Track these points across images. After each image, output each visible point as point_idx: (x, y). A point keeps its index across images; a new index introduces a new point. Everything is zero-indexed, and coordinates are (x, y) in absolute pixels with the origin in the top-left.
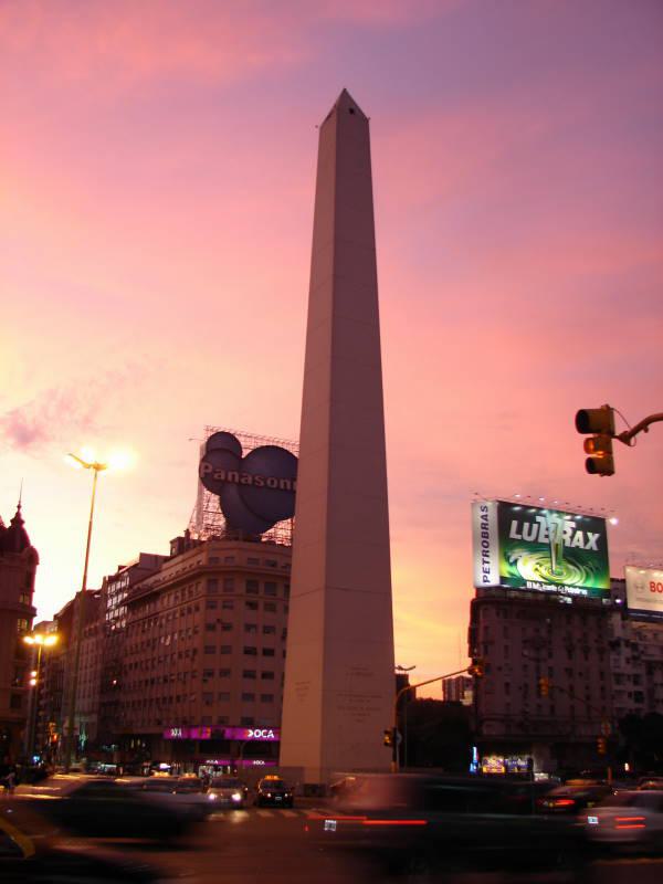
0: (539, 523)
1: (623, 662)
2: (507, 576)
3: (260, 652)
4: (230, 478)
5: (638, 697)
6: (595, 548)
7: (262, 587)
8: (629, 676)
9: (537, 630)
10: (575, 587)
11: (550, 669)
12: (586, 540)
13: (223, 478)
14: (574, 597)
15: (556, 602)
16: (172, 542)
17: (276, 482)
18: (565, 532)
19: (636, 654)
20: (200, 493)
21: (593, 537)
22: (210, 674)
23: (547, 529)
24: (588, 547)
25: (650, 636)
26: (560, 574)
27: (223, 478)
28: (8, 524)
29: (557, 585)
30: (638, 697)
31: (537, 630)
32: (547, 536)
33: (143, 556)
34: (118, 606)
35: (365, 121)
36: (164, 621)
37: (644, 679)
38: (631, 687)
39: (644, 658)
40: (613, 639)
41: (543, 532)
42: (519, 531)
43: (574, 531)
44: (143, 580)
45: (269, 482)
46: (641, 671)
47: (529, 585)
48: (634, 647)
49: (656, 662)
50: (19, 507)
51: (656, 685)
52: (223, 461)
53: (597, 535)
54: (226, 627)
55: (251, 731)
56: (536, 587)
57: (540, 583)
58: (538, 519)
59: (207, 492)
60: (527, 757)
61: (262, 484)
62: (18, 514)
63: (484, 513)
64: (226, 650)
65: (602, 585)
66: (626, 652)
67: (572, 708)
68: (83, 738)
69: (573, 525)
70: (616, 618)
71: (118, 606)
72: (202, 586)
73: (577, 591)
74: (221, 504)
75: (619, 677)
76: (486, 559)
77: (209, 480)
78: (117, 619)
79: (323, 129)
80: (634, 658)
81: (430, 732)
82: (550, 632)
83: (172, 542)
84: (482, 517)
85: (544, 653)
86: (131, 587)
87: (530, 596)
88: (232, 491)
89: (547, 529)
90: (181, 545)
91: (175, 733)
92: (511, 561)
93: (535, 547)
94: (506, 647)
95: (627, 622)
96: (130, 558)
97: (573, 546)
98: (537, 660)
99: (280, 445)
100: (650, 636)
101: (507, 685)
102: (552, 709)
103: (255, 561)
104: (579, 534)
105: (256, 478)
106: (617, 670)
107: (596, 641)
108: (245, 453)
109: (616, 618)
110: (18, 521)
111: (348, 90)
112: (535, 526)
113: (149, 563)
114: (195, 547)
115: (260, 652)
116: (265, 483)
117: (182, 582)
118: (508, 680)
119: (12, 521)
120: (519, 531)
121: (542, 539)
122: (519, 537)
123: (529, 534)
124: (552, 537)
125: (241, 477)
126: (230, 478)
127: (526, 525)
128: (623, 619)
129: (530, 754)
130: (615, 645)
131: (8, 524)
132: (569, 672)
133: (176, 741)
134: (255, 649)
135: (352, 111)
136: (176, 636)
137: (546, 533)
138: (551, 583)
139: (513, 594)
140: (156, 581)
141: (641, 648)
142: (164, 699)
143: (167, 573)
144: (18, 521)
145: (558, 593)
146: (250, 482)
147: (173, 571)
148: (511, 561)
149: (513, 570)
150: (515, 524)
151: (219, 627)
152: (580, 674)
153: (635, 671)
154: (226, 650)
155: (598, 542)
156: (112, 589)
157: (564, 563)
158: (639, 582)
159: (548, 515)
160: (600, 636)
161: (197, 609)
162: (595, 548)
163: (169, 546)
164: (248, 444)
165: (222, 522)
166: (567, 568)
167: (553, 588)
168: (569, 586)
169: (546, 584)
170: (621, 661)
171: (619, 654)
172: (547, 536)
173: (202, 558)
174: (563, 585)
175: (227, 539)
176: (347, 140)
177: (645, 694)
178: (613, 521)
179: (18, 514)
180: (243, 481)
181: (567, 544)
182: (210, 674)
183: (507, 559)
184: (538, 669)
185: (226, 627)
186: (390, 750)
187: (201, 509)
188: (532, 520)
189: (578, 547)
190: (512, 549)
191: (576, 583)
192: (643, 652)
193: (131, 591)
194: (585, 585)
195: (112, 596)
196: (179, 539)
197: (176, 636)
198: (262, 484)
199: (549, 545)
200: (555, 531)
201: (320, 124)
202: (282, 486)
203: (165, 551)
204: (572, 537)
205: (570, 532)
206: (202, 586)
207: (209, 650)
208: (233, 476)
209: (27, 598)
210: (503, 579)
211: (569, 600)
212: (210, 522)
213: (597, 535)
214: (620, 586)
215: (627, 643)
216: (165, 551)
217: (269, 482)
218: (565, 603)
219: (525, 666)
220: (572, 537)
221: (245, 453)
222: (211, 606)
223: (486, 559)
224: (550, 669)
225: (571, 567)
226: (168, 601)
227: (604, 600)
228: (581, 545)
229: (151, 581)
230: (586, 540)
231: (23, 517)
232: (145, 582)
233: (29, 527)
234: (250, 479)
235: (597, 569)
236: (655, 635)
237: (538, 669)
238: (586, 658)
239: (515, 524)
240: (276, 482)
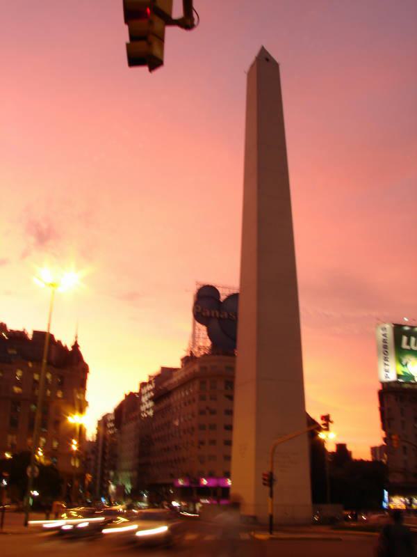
2: (402, 374)
4: (213, 315)
20: (194, 325)
22: (202, 443)
28: (70, 349)
33: (163, 369)
34: (148, 401)
35: (276, 66)
42: (408, 343)
50: (76, 337)
52: (210, 307)
54: (213, 412)
59: (198, 324)
62: (76, 343)
63: (383, 332)
64: (213, 427)
68: (129, 487)
72: (197, 382)
74: (209, 335)
76: (387, 363)
77: (199, 316)
78: (148, 409)
79: (249, 74)
81: (338, 479)
90: (187, 360)
91: (181, 482)
96: (155, 370)
105: (231, 315)
108: (223, 298)
110: (76, 346)
111: (265, 48)
113: (166, 373)
117: (184, 384)
119: (73, 347)
120: (408, 343)
125: (220, 313)
126: (213, 315)
131: (70, 349)
133: (182, 487)
135: (267, 60)
136: (182, 420)
139: (406, 386)
142: (175, 460)
143: (176, 379)
144: (76, 346)
147: (179, 377)
149: (405, 370)
150: (405, 339)
151: (207, 412)
154: (213, 427)
156: (144, 391)
161: (194, 400)
165: (208, 343)
173: (196, 367)
175: (213, 354)
176: (265, 78)
179: (76, 343)
180: (222, 316)
182: (202, 443)
185: (213, 412)
186: (267, 489)
187: (194, 336)
190: (407, 354)
195: (144, 395)
197: (182, 420)
201: (247, 67)
203: (176, 364)
206: (197, 382)
207: (202, 427)
208: (215, 314)
209: (82, 395)
210: (399, 376)
212: (201, 344)
216: (176, 364)
221: (223, 298)
222: (202, 398)
223: (387, 363)
226: (177, 397)
229: (166, 384)
231: (79, 343)
233: (82, 350)
234: (226, 315)
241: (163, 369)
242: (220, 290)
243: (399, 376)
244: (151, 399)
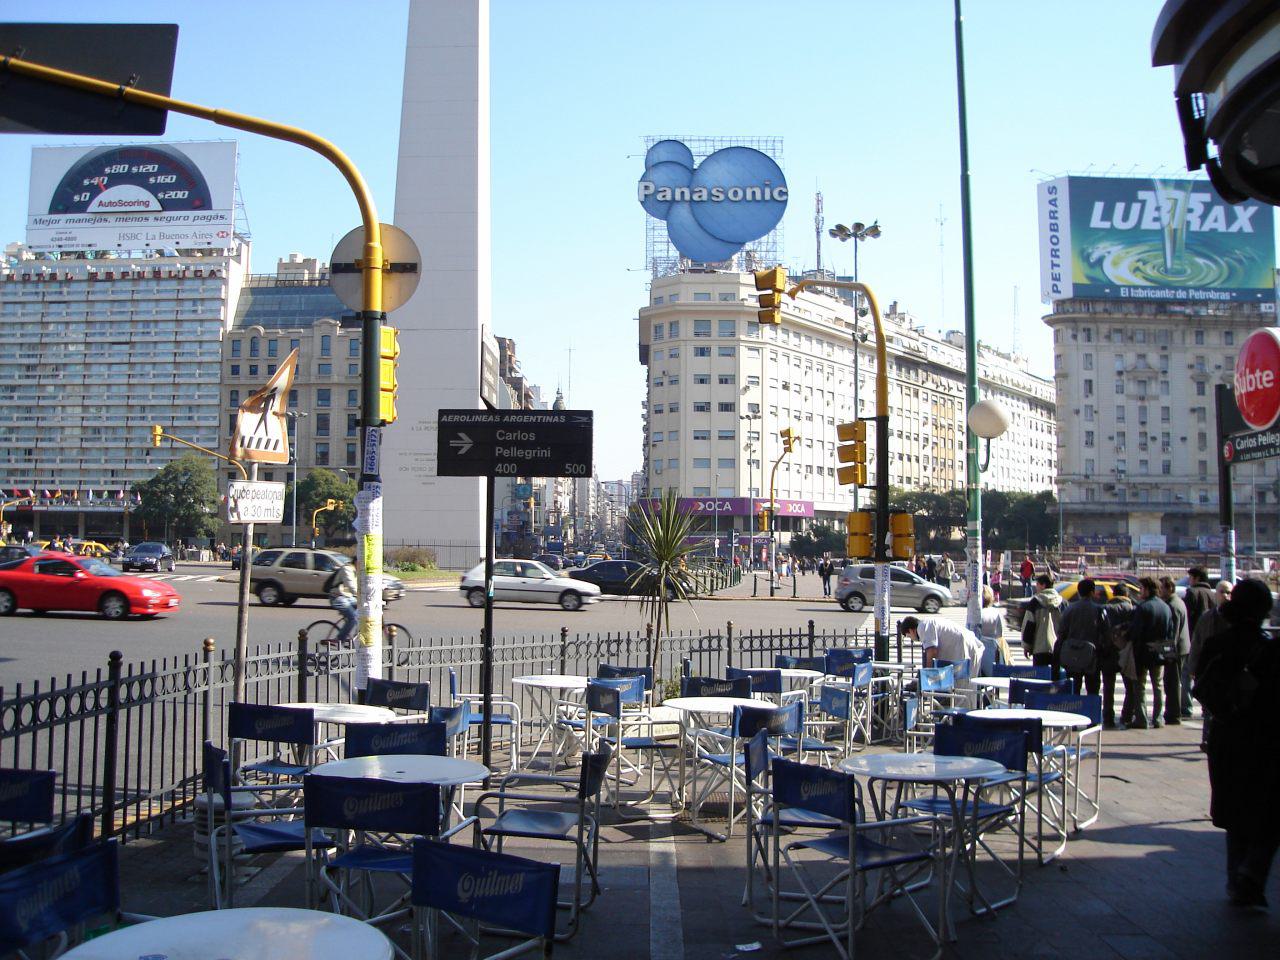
0: (1143, 203)
4: (678, 197)
6: (1248, 229)
7: (715, 328)
11: (1166, 409)
13: (669, 198)
17: (740, 193)
18: (1190, 211)
23: (1158, 209)
24: (1234, 228)
27: (669, 198)
31: (1142, 356)
32: (1156, 219)
45: (731, 195)
47: (1123, 293)
61: (722, 197)
63: (1053, 197)
76: (1056, 261)
77: (653, 204)
84: (1050, 202)
85: (1154, 388)
88: (682, 213)
89: (1158, 209)
94: (1089, 383)
97: (1206, 228)
101: (1090, 434)
103: (708, 296)
105: (714, 192)
108: (698, 161)
116: (725, 193)
118: (1090, 427)
121: (1148, 224)
122: (1107, 225)
123: (1125, 218)
124: (1165, 218)
126: (678, 197)
137: (1156, 214)
138: (1162, 286)
146: (705, 198)
149: (1096, 273)
155: (1252, 219)
162: (1248, 229)
164: (703, 149)
167: (1166, 294)
169: (1152, 288)
172: (1156, 219)
174: (1186, 289)
180: (696, 197)
181: (1195, 227)
184: (1143, 410)
189: (1213, 231)
190: (1101, 239)
194: (1226, 286)
198: (722, 197)
199: (1161, 231)
202: (749, 197)
205: (1199, 210)
217: (731, 195)
219: (1121, 408)
220: (1203, 217)
221: (698, 161)
223: (1056, 261)
224: (1166, 409)
228: (1221, 227)
230: (1231, 218)
237: (1143, 410)
239: (1099, 207)
240: (740, 193)
242: (694, 148)
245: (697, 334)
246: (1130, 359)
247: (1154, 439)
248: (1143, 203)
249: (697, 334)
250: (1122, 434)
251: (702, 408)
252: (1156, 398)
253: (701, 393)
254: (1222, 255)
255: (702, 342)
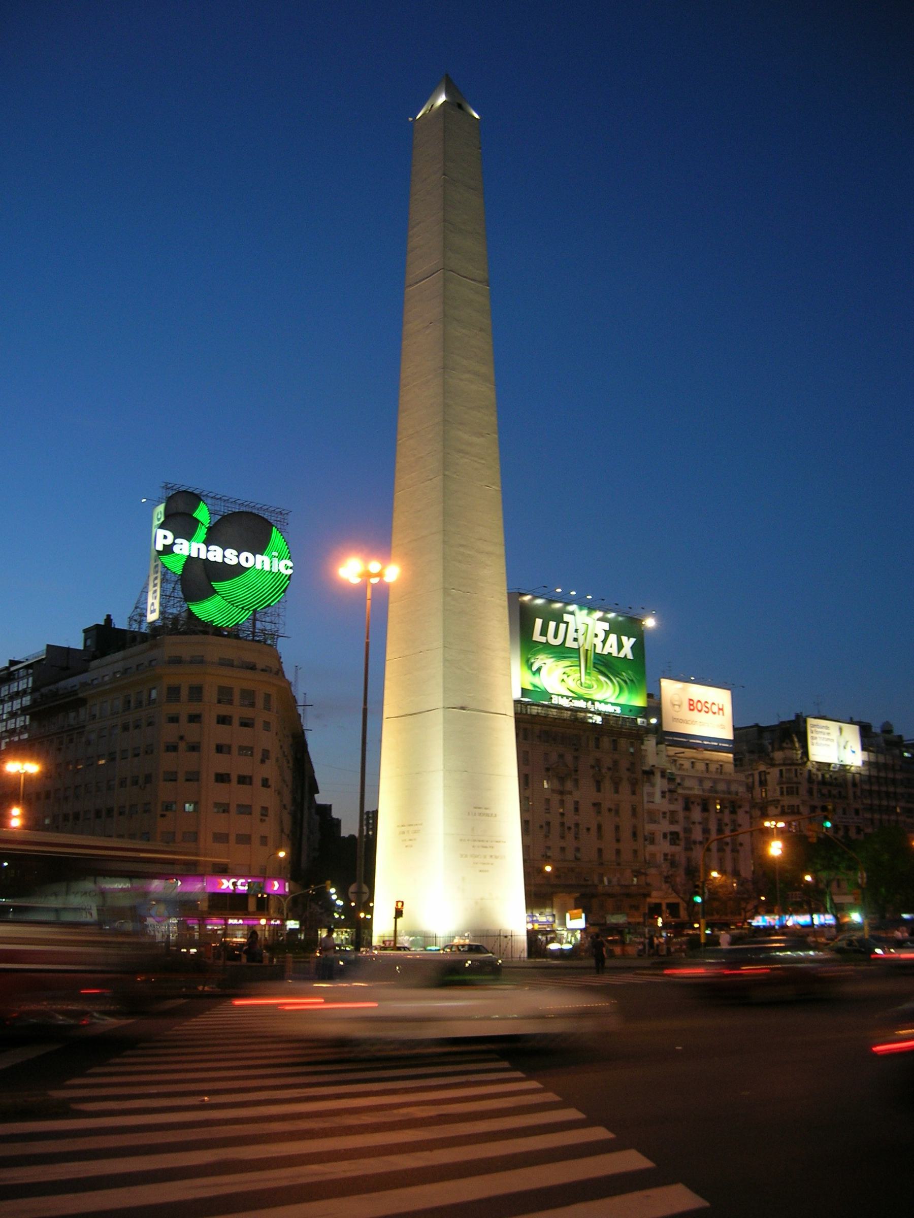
0: (567, 623)
1: (658, 795)
2: (531, 688)
3: (234, 779)
5: (674, 838)
6: (630, 656)
8: (664, 813)
9: (561, 756)
10: (606, 703)
12: (620, 646)
14: (606, 716)
15: (584, 722)
16: (85, 631)
19: (672, 787)
21: (628, 642)
23: (576, 631)
24: (622, 655)
25: (687, 764)
26: (590, 687)
29: (587, 700)
30: (674, 838)
32: (575, 640)
33: (49, 647)
36: (93, 736)
37: (681, 815)
38: (665, 826)
39: (680, 791)
40: (646, 768)
41: (571, 634)
42: (544, 632)
43: (607, 633)
44: (57, 682)
46: (678, 806)
47: (555, 700)
48: (671, 779)
49: (696, 796)
51: (694, 823)
53: (633, 640)
54: (194, 748)
55: (224, 881)
56: (565, 703)
57: (568, 697)
58: (566, 617)
60: (548, 910)
65: (639, 701)
66: (660, 784)
67: (600, 851)
69: (606, 626)
70: (650, 744)
71: (13, 715)
73: (609, 709)
75: (652, 817)
80: (670, 791)
82: (576, 758)
83: (86, 631)
85: (569, 785)
86: (35, 689)
87: (554, 712)
89: (576, 631)
92: (535, 668)
93: (561, 652)
95: (662, 747)
97: (605, 652)
98: (562, 793)
99: (256, 512)
100: (687, 764)
102: (578, 849)
104: (613, 638)
106: (651, 806)
107: (628, 770)
109: (650, 744)
112: (562, 627)
114: (143, 642)
115: (234, 779)
120: (544, 632)
121: (570, 643)
123: (556, 636)
124: (581, 639)
127: (552, 625)
128: (657, 744)
129: (552, 907)
130: (650, 773)
132: (597, 805)
134: (228, 775)
138: (579, 698)
139: (535, 710)
140: (84, 685)
141: (678, 780)
145: (586, 710)
148: (535, 668)
149: (536, 680)
150: (539, 622)
152: (610, 810)
153: (672, 807)
155: (633, 648)
157: (594, 673)
158: (676, 698)
159: (577, 612)
160: (632, 764)
162: (630, 656)
163: (82, 636)
166: (598, 680)
167: (581, 704)
168: (600, 702)
170: (655, 794)
171: (653, 785)
172: (575, 640)
177: (682, 835)
178: (650, 623)
181: (598, 651)
183: (530, 666)
185: (194, 748)
188: (559, 619)
190: (538, 652)
191: (609, 698)
192: (679, 784)
193: (37, 695)
196: (97, 626)
200: (585, 634)
204: (604, 642)
205: (602, 636)
210: (524, 692)
211: (598, 719)
213: (633, 640)
214: (654, 707)
215: (663, 774)
216: (77, 642)
218: (595, 724)
220: (604, 642)
224: (577, 803)
225: (602, 678)
227: (639, 720)
228: (615, 654)
230: (620, 646)
232: (62, 684)
235: (632, 681)
236: (693, 763)
238: (617, 792)
241: (49, 647)
243: (524, 692)
244: (24, 710)
245: (219, 702)
246: (554, 757)
247: (569, 828)
248: (567, 623)
249: (219, 702)
250: (548, 824)
251: (222, 778)
252: (570, 793)
253: (221, 763)
254: (615, 676)
255: (224, 710)
